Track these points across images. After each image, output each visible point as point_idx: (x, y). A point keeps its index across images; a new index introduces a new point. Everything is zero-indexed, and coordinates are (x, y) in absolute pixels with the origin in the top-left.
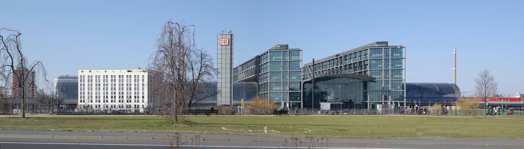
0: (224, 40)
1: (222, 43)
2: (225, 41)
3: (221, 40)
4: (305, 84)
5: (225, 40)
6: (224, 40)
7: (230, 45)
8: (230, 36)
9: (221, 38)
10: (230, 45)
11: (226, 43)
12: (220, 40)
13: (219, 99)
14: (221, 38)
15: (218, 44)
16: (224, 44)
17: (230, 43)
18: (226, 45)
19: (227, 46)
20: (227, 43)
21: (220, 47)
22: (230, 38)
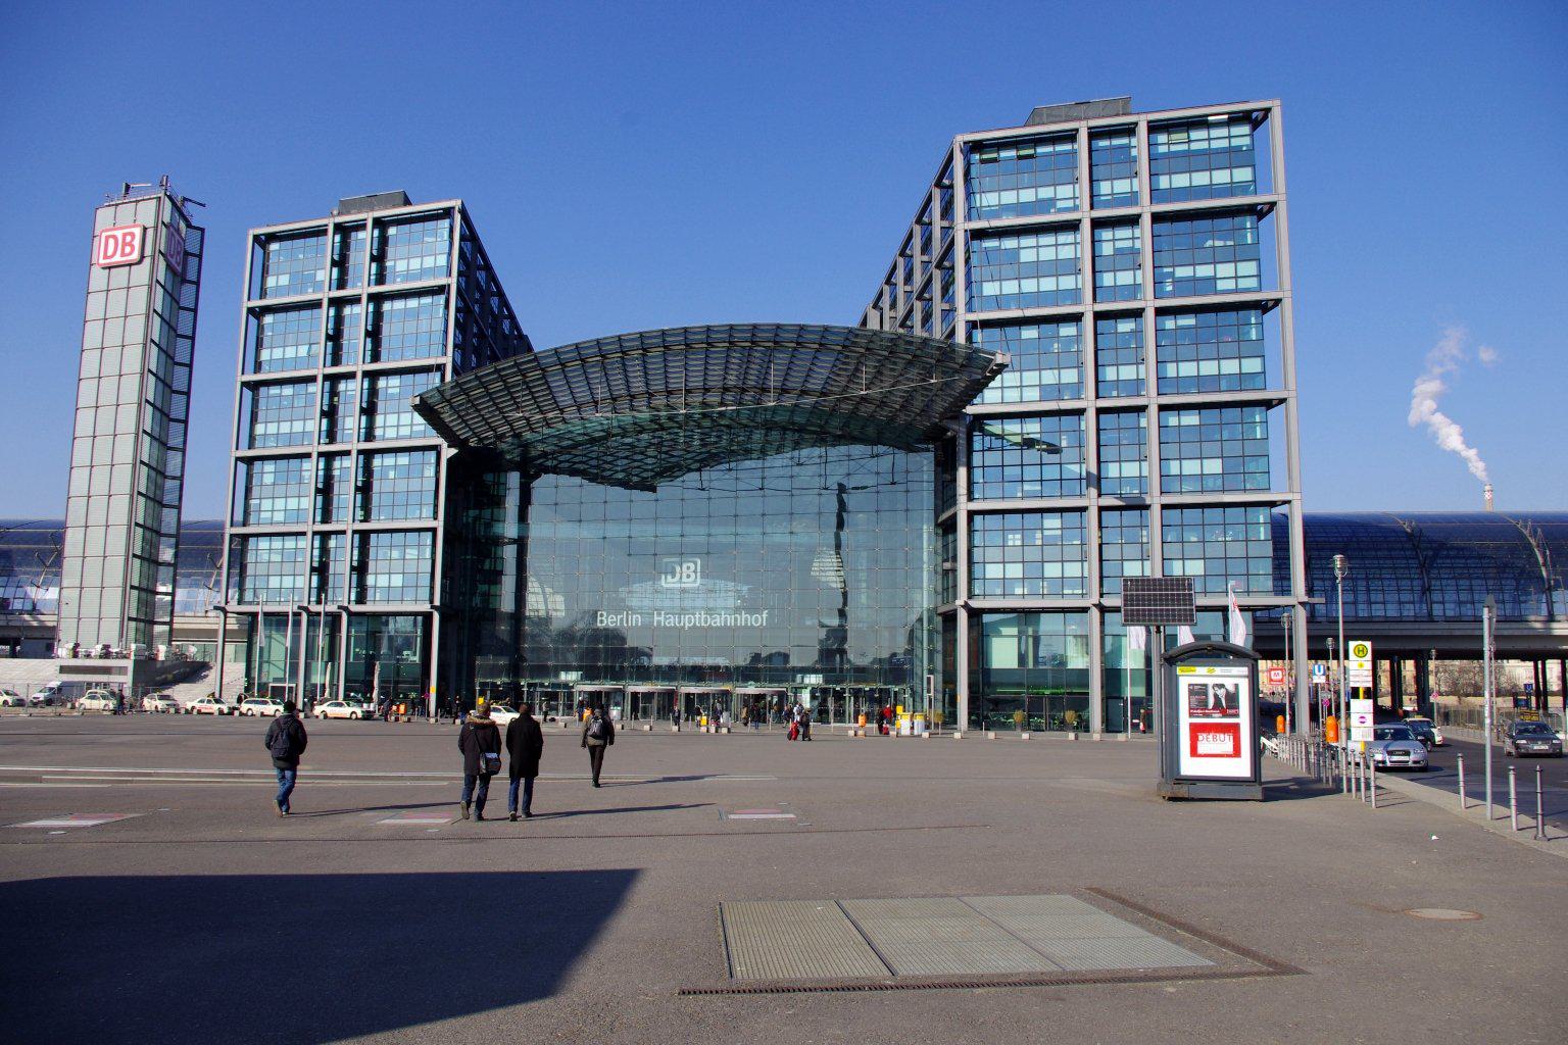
0: (119, 234)
1: (110, 253)
2: (124, 239)
3: (107, 238)
4: (537, 476)
5: (125, 235)
6: (119, 234)
7: (147, 261)
10: (147, 261)
11: (128, 249)
12: (104, 234)
16: (118, 259)
17: (148, 251)
18: (130, 265)
19: (133, 267)
20: (130, 254)
22: (150, 223)
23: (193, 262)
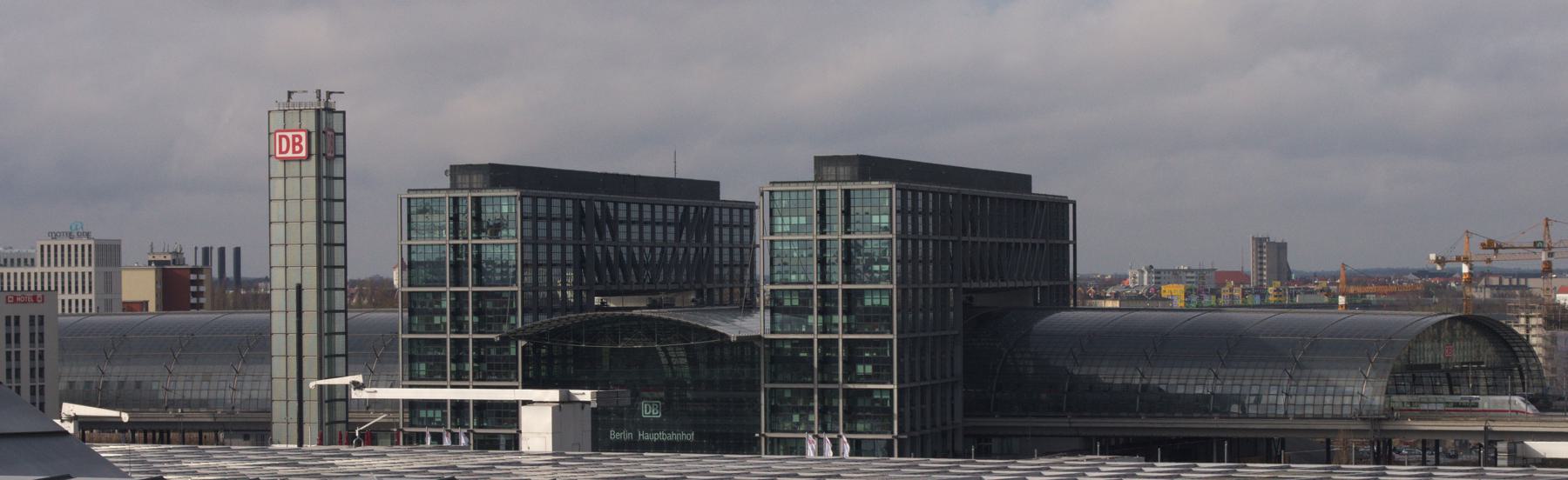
0: (290, 135)
1: (284, 149)
2: (294, 140)
3: (281, 137)
5: (294, 137)
7: (314, 158)
8: (312, 115)
9: (282, 128)
11: (297, 148)
12: (278, 134)
13: (1183, 289)
14: (282, 128)
15: (272, 153)
16: (290, 154)
17: (313, 150)
18: (300, 160)
21: (278, 169)
22: (312, 128)
23: (340, 139)
